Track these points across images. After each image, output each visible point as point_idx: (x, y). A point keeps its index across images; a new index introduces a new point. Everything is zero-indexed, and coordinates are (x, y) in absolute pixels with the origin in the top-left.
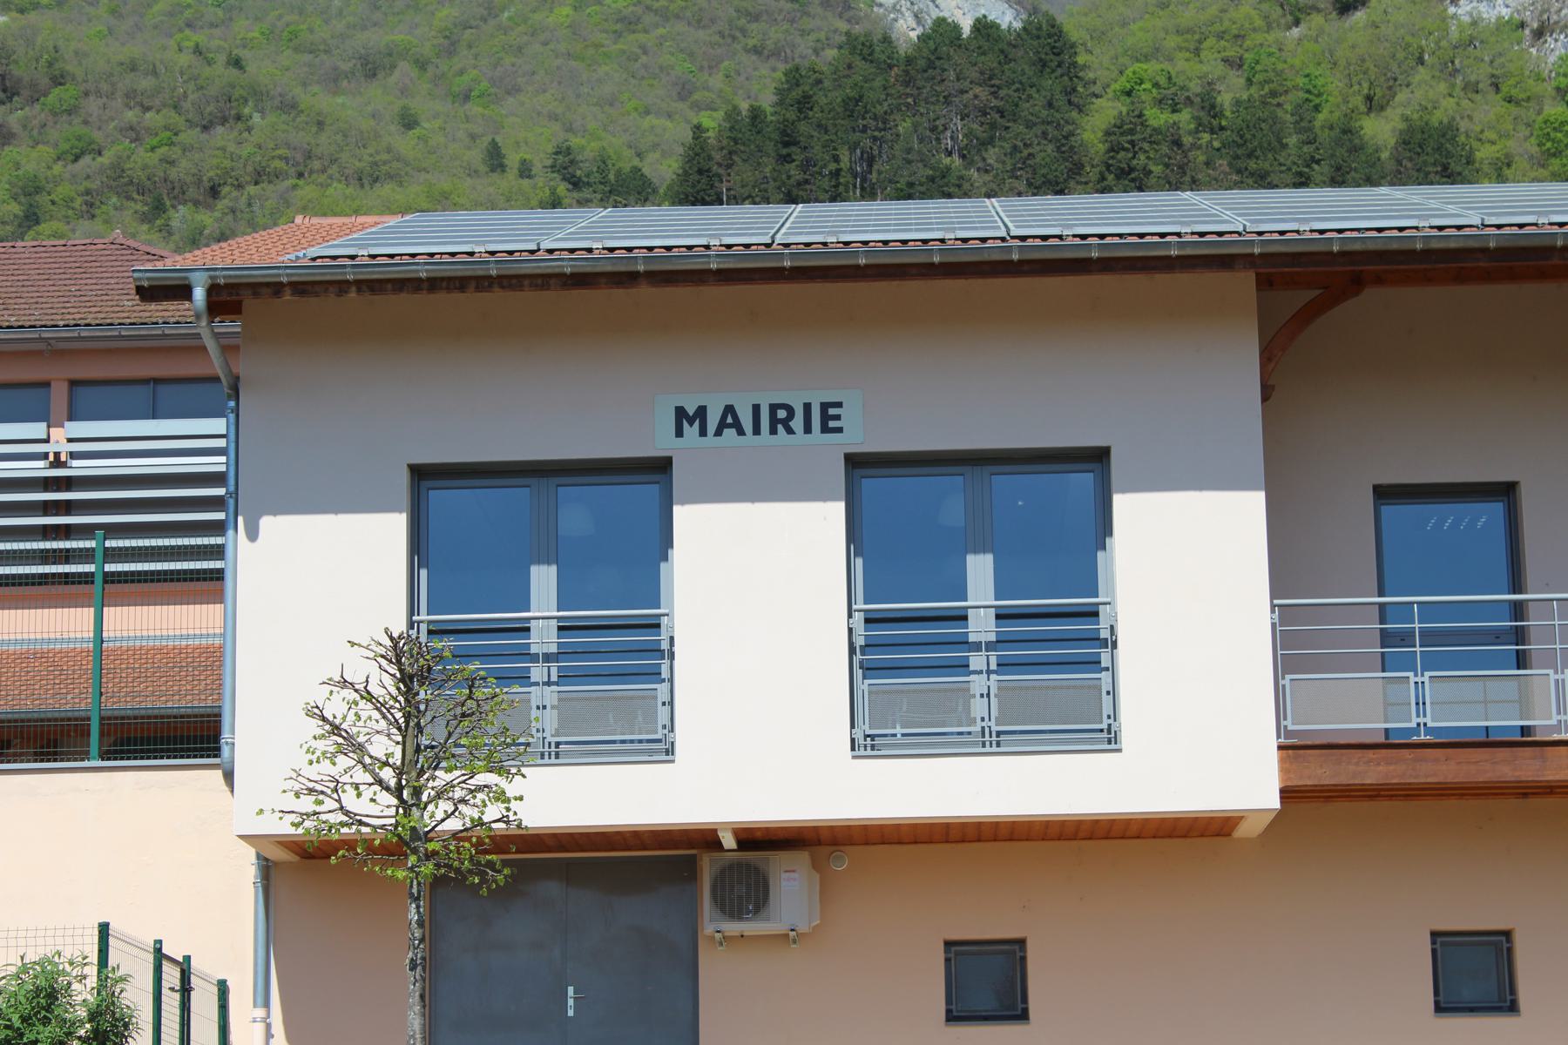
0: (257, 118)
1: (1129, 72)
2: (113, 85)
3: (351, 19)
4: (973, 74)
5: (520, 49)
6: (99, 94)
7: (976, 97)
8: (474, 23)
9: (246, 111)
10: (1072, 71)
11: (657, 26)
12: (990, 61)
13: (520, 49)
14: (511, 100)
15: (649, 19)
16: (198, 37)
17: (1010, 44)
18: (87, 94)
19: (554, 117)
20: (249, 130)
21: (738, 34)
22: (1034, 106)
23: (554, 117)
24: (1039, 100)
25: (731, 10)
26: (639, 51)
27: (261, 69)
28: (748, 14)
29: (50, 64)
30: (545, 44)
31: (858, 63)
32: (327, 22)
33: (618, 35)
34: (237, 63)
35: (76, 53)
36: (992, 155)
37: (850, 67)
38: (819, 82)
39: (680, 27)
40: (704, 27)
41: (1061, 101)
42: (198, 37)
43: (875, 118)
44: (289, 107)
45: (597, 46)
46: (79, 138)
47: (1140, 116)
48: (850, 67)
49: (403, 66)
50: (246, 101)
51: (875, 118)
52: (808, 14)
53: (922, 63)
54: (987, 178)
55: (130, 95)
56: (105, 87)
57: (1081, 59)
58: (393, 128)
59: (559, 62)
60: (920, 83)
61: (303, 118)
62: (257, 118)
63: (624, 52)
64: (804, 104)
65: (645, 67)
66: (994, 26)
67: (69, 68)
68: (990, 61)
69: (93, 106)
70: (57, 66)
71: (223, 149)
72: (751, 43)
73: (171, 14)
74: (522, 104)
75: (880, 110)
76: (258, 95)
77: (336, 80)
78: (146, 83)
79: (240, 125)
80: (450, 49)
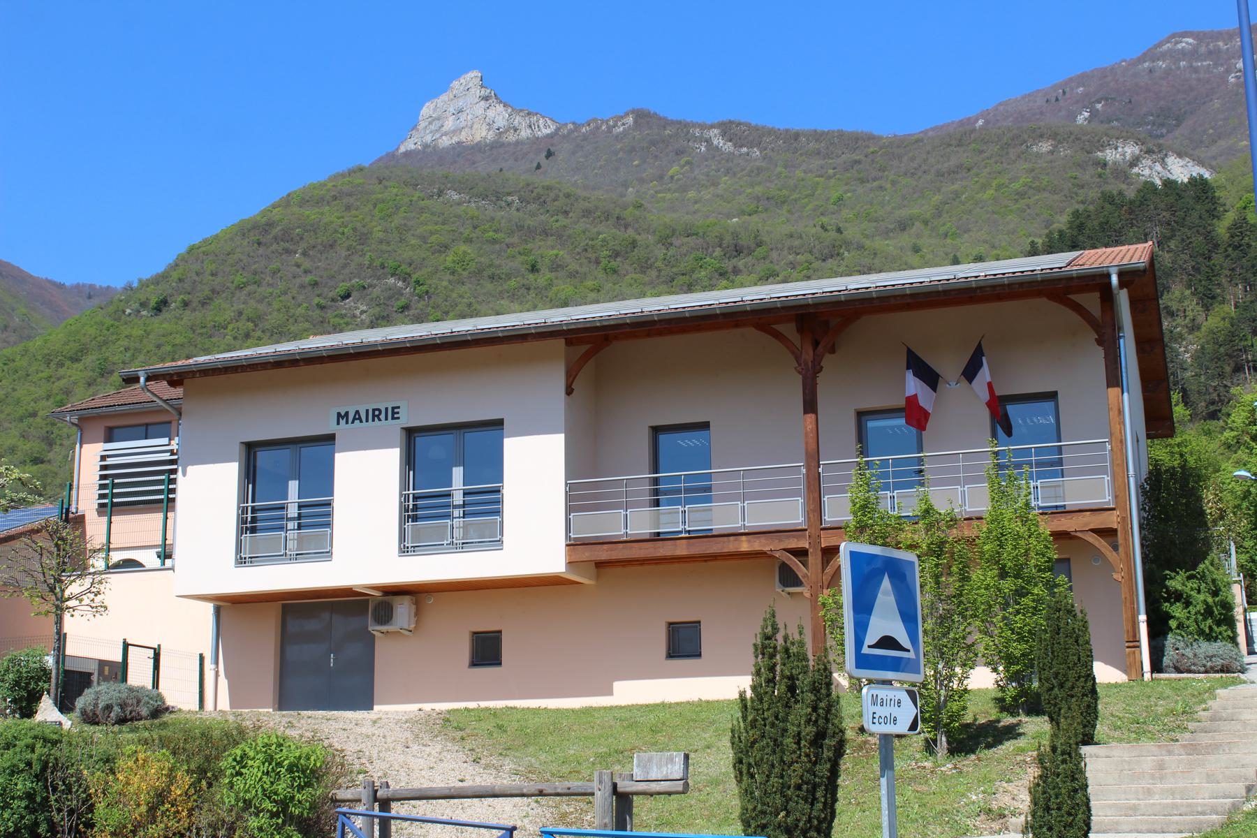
0: (846, 254)
1: (1244, 198)
2: (783, 244)
3: (893, 205)
4: (1162, 206)
5: (970, 211)
6: (777, 249)
7: (1164, 217)
8: (949, 201)
9: (842, 251)
10: (1214, 200)
11: (1034, 195)
12: (1171, 199)
13: (970, 211)
14: (966, 235)
15: (1031, 192)
16: (825, 220)
17: (1182, 190)
18: (772, 250)
19: (986, 242)
20: (843, 259)
21: (1073, 195)
22: (1194, 218)
23: (986, 242)
24: (1195, 214)
25: (1070, 185)
26: (1026, 207)
27: (851, 233)
28: (1078, 185)
29: (755, 238)
30: (982, 208)
31: (1107, 206)
32: (883, 207)
33: (1017, 201)
34: (839, 230)
35: (767, 232)
36: (1172, 244)
37: (1103, 208)
38: (1089, 216)
39: (1046, 194)
40: (1057, 194)
41: (1205, 215)
42: (825, 220)
43: (1115, 231)
44: (860, 247)
45: (1006, 207)
46: (769, 270)
47: (1244, 219)
48: (1103, 208)
49: (917, 224)
50: (841, 247)
51: (1115, 231)
52: (1107, 183)
53: (1138, 203)
54: (1171, 255)
55: (790, 248)
56: (779, 246)
57: (1217, 194)
58: (909, 253)
59: (988, 216)
60: (1137, 213)
61: (867, 252)
62: (846, 254)
63: (1019, 209)
64: (1081, 227)
65: (1029, 214)
66: (1175, 182)
67: (764, 239)
68: (1171, 199)
69: (774, 255)
70: (759, 238)
71: (831, 269)
72: (1080, 199)
73: (814, 210)
74: (971, 236)
75: (1117, 227)
76: (847, 244)
77: (887, 233)
78: (797, 243)
79: (839, 258)
80: (939, 214)
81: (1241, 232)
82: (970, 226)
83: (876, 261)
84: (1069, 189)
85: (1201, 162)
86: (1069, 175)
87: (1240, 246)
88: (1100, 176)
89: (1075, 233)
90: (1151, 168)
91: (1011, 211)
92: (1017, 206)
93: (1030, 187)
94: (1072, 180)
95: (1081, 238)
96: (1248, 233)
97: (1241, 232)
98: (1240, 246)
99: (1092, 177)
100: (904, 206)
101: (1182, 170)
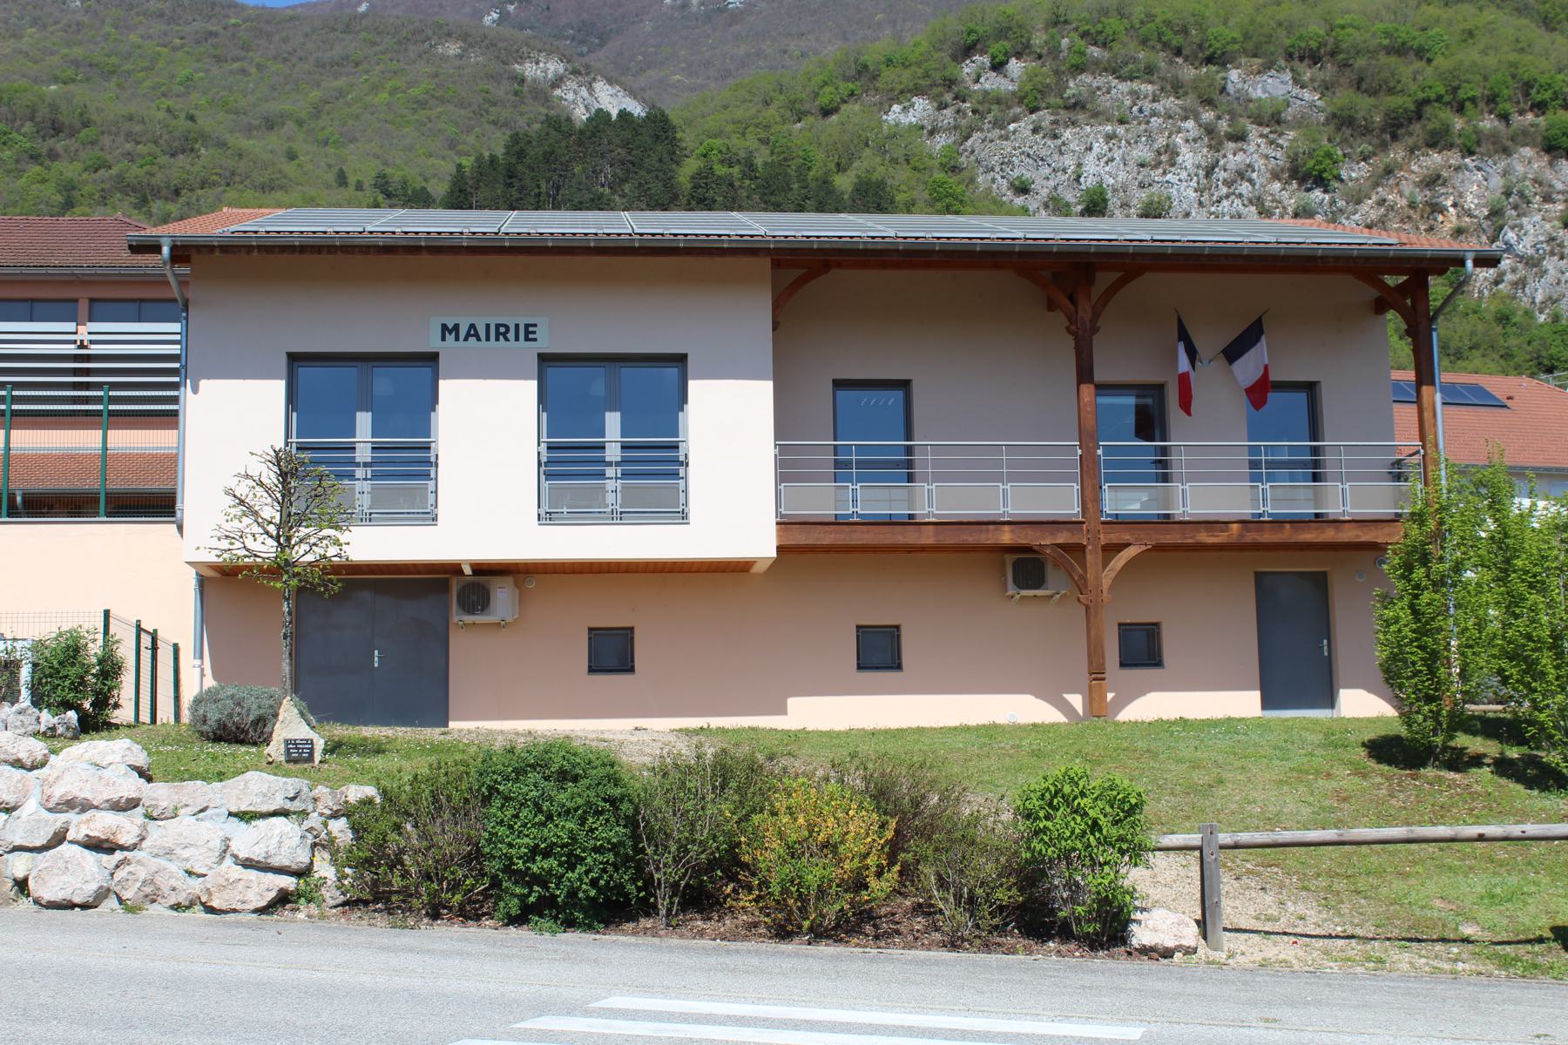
0: (203, 151)
1: (705, 144)
2: (119, 128)
4: (617, 141)
5: (357, 116)
6: (110, 133)
7: (619, 154)
9: (197, 146)
10: (673, 142)
11: (437, 106)
12: (628, 134)
13: (357, 116)
15: (433, 102)
16: (169, 103)
17: (638, 124)
18: (103, 133)
19: (377, 156)
20: (198, 157)
22: (652, 161)
23: (377, 156)
25: (481, 99)
27: (205, 122)
29: (81, 115)
30: (372, 114)
31: (553, 132)
33: (415, 111)
34: (192, 118)
35: (97, 109)
36: (627, 188)
37: (547, 134)
38: (530, 142)
39: (451, 107)
40: (465, 108)
41: (666, 158)
42: (169, 103)
43: (561, 164)
44: (222, 144)
45: (402, 116)
46: (98, 159)
47: (711, 169)
48: (547, 134)
49: (290, 124)
50: (197, 141)
51: (561, 164)
52: (524, 103)
53: (588, 134)
54: (624, 200)
55: (128, 135)
56: (114, 129)
57: (678, 135)
58: (282, 160)
59: (379, 125)
60: (587, 145)
61: (230, 151)
62: (203, 151)
63: (418, 120)
64: (521, 155)
65: (430, 129)
66: (631, 114)
67: (92, 117)
69: (106, 140)
70: (86, 116)
72: (491, 118)
73: (154, 88)
74: (358, 148)
75: (564, 159)
76: (204, 137)
77: (250, 130)
78: (138, 128)
79: (193, 155)
81: (706, 184)
82: (357, 135)
83: (242, 164)
84: (479, 106)
85: (633, 94)
86: (480, 87)
87: (705, 199)
88: (516, 94)
89: (513, 160)
90: (575, 92)
91: (408, 122)
92: (416, 117)
93: (433, 96)
94: (483, 94)
95: (520, 167)
96: (714, 186)
97: (706, 184)
98: (705, 199)
99: (507, 93)
100: (274, 99)
101: (611, 99)
